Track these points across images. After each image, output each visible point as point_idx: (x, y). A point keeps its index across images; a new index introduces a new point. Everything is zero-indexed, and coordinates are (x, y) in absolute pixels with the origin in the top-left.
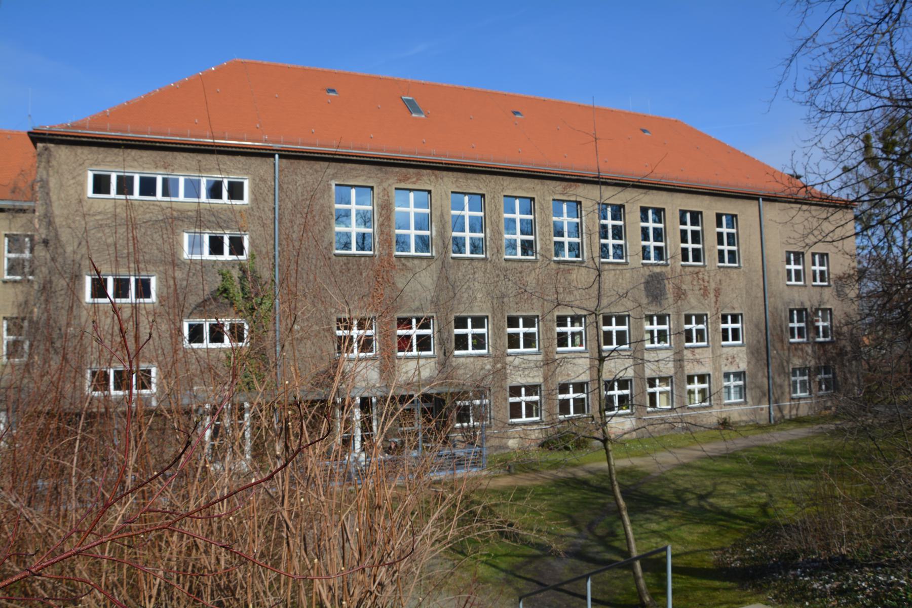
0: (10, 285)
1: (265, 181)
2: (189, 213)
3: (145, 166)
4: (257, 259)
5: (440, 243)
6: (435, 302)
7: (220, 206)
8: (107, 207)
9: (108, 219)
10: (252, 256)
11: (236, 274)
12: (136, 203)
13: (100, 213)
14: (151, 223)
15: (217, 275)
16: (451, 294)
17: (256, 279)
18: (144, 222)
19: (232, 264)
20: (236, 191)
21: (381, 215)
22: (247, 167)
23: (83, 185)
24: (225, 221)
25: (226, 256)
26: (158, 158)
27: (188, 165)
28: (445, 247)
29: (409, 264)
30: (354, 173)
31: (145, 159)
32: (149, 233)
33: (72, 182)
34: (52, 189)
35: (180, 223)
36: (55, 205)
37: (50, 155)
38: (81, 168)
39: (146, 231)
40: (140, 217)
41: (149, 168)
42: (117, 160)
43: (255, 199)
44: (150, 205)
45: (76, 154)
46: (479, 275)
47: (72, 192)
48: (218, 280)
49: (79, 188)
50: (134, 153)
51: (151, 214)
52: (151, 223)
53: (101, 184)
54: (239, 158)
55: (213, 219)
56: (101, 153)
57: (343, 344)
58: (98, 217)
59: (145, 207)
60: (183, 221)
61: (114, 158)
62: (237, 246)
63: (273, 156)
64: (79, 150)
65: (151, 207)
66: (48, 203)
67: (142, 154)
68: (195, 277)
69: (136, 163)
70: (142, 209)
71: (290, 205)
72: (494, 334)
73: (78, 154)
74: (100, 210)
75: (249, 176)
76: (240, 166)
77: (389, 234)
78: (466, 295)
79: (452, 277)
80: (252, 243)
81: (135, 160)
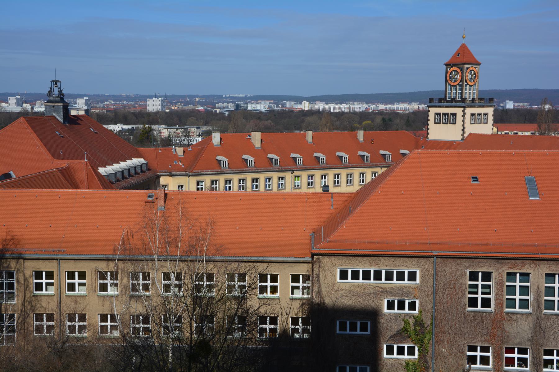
1: (428, 271)
2: (388, 289)
3: (365, 265)
4: (423, 313)
5: (536, 305)
6: (532, 340)
7: (404, 285)
8: (346, 287)
9: (347, 292)
10: (420, 312)
11: (411, 321)
12: (361, 284)
13: (343, 290)
14: (368, 294)
15: (402, 321)
16: (542, 335)
18: (365, 294)
19: (410, 316)
20: (412, 276)
21: (497, 288)
22: (418, 264)
23: (335, 276)
24: (406, 293)
25: (407, 311)
26: (372, 261)
27: (387, 264)
28: (539, 307)
29: (514, 317)
30: (481, 264)
31: (365, 262)
32: (367, 300)
33: (330, 274)
34: (321, 279)
35: (383, 294)
36: (322, 286)
37: (320, 262)
38: (334, 267)
39: (366, 299)
40: (363, 291)
41: (367, 266)
42: (351, 262)
43: (422, 282)
44: (367, 285)
45: (332, 260)
47: (330, 279)
48: (402, 324)
49: (333, 277)
50: (359, 258)
51: (368, 290)
52: (368, 294)
53: (344, 274)
54: (414, 259)
55: (400, 292)
56: (344, 259)
58: (342, 292)
59: (365, 286)
60: (384, 293)
61: (350, 262)
62: (412, 306)
63: (433, 257)
64: (333, 258)
65: (368, 286)
66: (320, 286)
67: (363, 259)
68: (390, 322)
69: (360, 264)
70: (363, 287)
71: (442, 284)
73: (333, 260)
74: (343, 288)
75: (420, 269)
76: (415, 263)
77: (501, 300)
78: (553, 337)
79: (543, 326)
80: (420, 305)
81: (360, 262)
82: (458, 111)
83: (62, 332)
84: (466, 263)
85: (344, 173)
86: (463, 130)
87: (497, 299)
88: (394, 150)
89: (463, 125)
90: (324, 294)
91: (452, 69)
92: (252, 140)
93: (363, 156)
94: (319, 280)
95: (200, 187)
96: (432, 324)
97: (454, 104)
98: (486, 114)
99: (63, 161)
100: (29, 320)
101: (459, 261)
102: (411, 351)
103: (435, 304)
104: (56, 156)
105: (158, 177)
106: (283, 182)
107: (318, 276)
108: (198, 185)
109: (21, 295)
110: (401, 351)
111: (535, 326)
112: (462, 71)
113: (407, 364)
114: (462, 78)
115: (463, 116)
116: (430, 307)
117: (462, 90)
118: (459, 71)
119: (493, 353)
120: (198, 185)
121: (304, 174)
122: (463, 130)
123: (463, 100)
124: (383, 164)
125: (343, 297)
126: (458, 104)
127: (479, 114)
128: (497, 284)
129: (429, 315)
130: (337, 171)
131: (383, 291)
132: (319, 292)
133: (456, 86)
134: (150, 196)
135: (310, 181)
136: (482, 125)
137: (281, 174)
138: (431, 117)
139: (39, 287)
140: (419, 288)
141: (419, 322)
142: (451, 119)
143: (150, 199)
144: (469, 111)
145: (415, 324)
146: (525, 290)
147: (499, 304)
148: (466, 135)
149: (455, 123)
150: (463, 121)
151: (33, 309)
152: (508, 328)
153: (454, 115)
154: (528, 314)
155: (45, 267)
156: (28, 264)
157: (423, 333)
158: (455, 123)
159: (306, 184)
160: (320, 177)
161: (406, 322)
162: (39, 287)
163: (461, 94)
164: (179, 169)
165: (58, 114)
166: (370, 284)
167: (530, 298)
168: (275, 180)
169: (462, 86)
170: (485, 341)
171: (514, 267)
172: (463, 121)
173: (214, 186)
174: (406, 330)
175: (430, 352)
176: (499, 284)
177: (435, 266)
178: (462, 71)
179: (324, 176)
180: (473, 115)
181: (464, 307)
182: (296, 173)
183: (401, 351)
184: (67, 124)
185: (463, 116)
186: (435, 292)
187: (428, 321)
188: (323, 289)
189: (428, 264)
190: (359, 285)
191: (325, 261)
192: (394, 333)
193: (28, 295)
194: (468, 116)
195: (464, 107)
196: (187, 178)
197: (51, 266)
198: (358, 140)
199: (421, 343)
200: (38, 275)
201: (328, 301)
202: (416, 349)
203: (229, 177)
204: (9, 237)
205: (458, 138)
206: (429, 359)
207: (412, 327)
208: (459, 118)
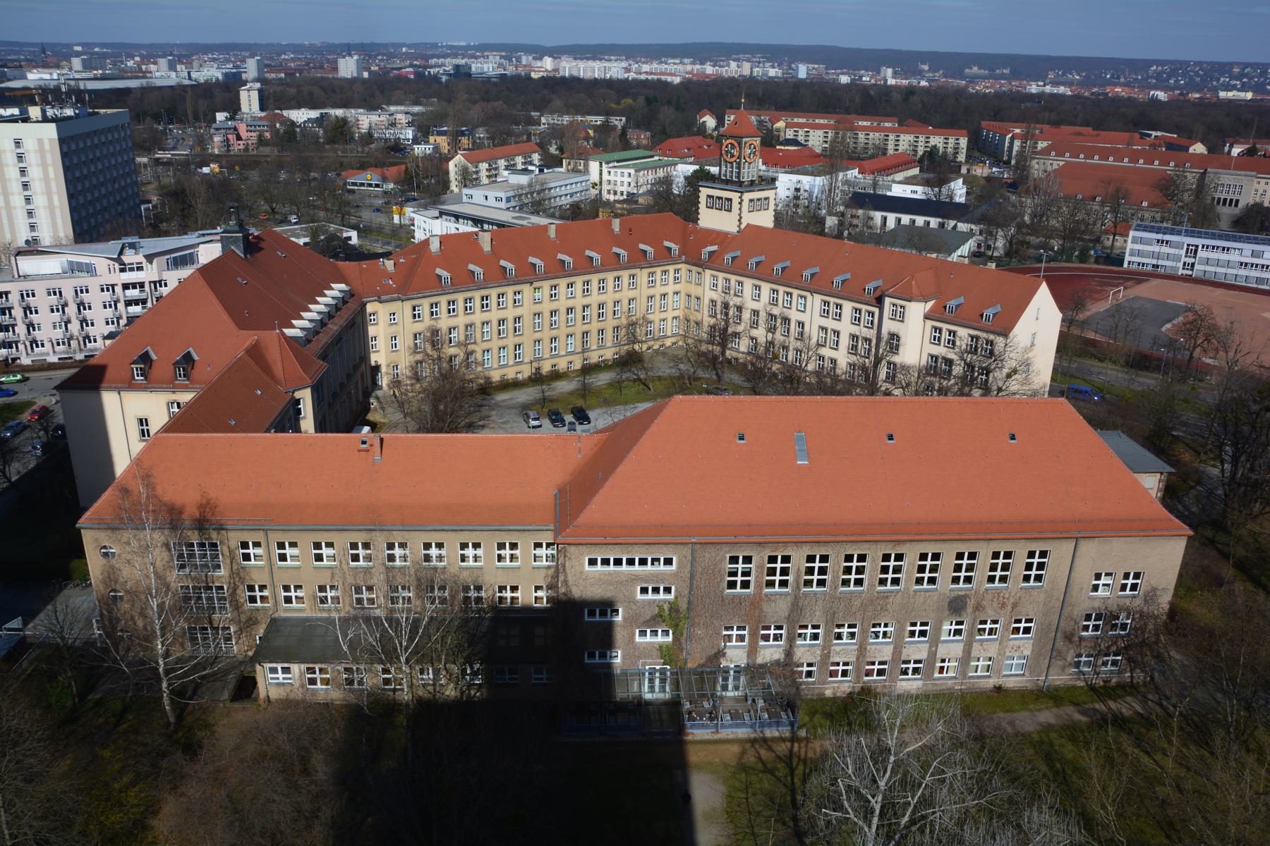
0: (501, 570)
5: (795, 586)
10: (676, 598)
11: (666, 607)
17: (677, 611)
19: (665, 601)
21: (757, 571)
29: (773, 598)
43: (679, 567)
46: (820, 602)
57: (729, 638)
62: (667, 590)
71: (700, 569)
72: (825, 634)
79: (800, 604)
80: (676, 591)
82: (735, 196)
83: (276, 603)
84: (726, 548)
85: (595, 278)
86: (739, 221)
87: (756, 581)
88: (656, 244)
89: (740, 215)
90: (570, 583)
91: (728, 141)
92: (480, 241)
93: (618, 255)
94: (564, 570)
95: (416, 312)
96: (688, 609)
97: (728, 187)
98: (766, 199)
99: (250, 332)
100: (239, 591)
101: (718, 547)
102: (666, 633)
103: (691, 590)
104: (242, 324)
105: (364, 305)
106: (520, 297)
107: (564, 566)
108: (414, 310)
109: (228, 567)
110: (655, 633)
111: (793, 605)
112: (740, 144)
113: (661, 647)
114: (740, 154)
115: (740, 203)
116: (686, 592)
117: (739, 168)
118: (736, 144)
119: (749, 631)
120: (414, 310)
121: (546, 285)
122: (739, 221)
123: (740, 184)
124: (643, 264)
125: (591, 585)
126: (734, 188)
127: (758, 200)
128: (757, 567)
129: (686, 600)
130: (586, 278)
131: (636, 578)
132: (566, 582)
133: (732, 163)
134: (364, 443)
135: (553, 292)
136: (762, 212)
137: (517, 288)
138: (703, 199)
139: (247, 557)
140: (675, 575)
141: (674, 608)
142: (725, 205)
143: (364, 446)
144: (747, 196)
145: (670, 610)
146: (785, 572)
147: (759, 586)
148: (743, 226)
149: (730, 210)
150: (740, 209)
151: (242, 580)
152: (766, 607)
153: (730, 200)
154: (786, 594)
155: (250, 538)
156: (231, 534)
157: (678, 618)
158: (730, 210)
159: (548, 297)
160: (566, 286)
161: (661, 608)
162: (247, 557)
163: (739, 173)
164: (388, 290)
165: (237, 247)
166: (621, 572)
167: (790, 578)
168: (510, 296)
169: (739, 164)
170: (743, 621)
171: (776, 550)
172: (740, 209)
173: (434, 310)
174: (661, 616)
175: (685, 635)
176: (760, 567)
177: (693, 552)
178: (740, 144)
179: (570, 285)
180: (751, 201)
181: (722, 592)
182: (536, 284)
183: (655, 633)
184: (249, 256)
185: (740, 203)
186: (692, 577)
187: (683, 606)
188: (570, 578)
189: (687, 551)
190: (610, 573)
191: (572, 549)
192: (648, 618)
193: (235, 567)
194: (745, 203)
195: (742, 192)
196: (400, 302)
197: (259, 537)
198: (613, 230)
199: (676, 627)
200: (245, 545)
201: (577, 593)
202: (671, 632)
203: (451, 297)
204: (204, 501)
205: (734, 229)
206: (683, 640)
207: (667, 612)
208: (735, 205)
